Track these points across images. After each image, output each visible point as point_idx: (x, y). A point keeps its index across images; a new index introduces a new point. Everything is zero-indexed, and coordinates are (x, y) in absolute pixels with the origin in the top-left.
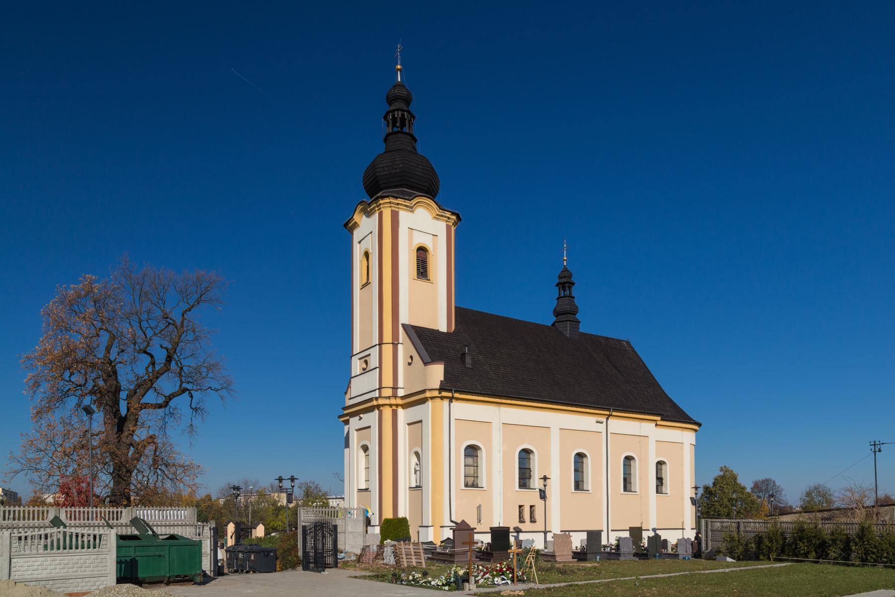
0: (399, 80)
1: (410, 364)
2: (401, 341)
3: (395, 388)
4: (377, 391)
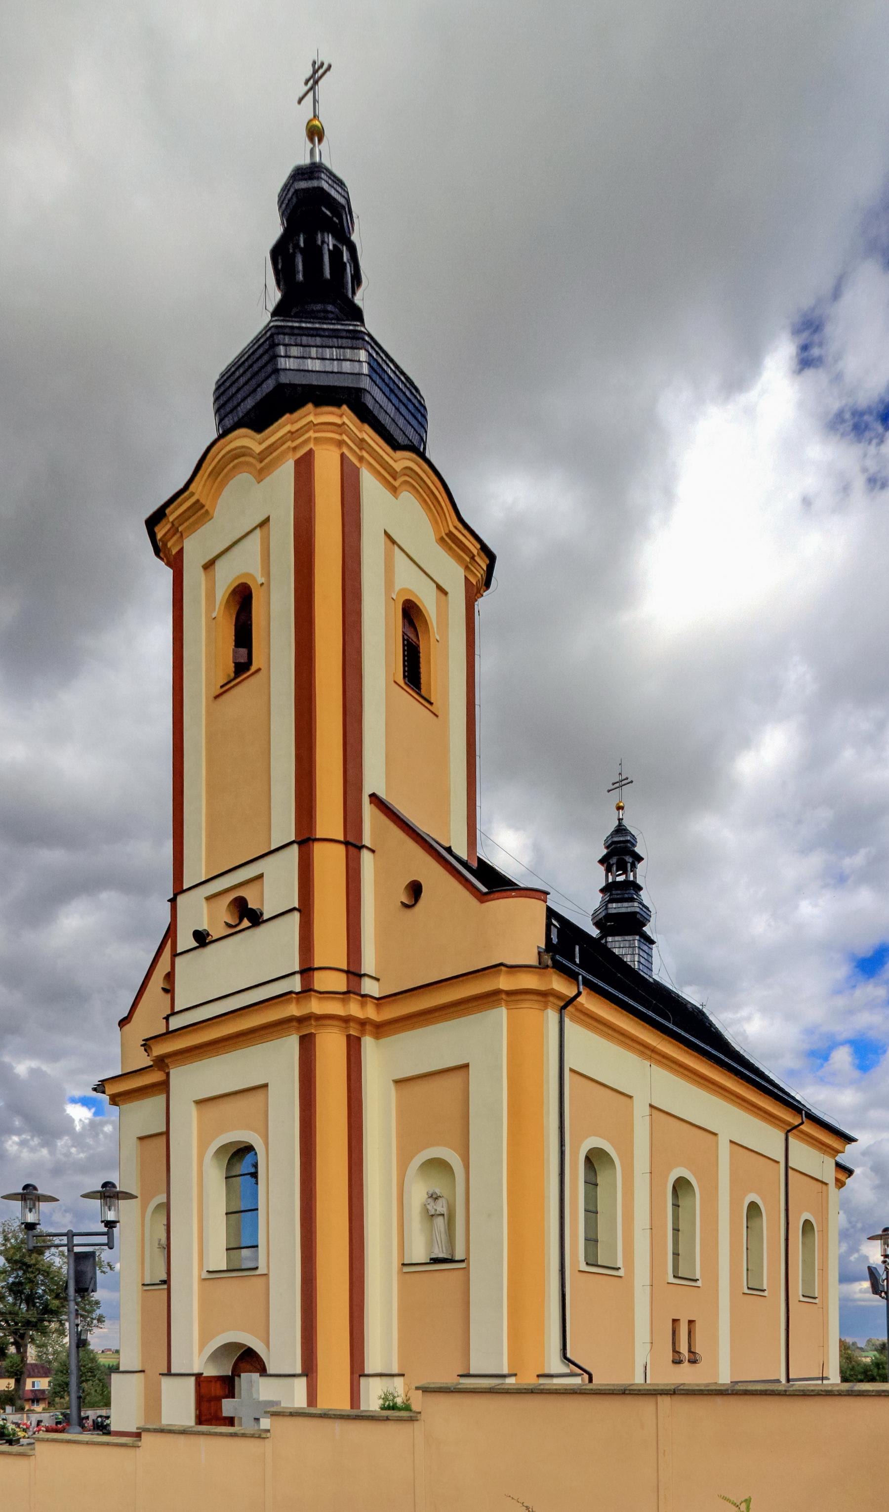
0: (324, 209)
1: (406, 906)
2: (367, 841)
3: (354, 974)
4: (298, 977)
